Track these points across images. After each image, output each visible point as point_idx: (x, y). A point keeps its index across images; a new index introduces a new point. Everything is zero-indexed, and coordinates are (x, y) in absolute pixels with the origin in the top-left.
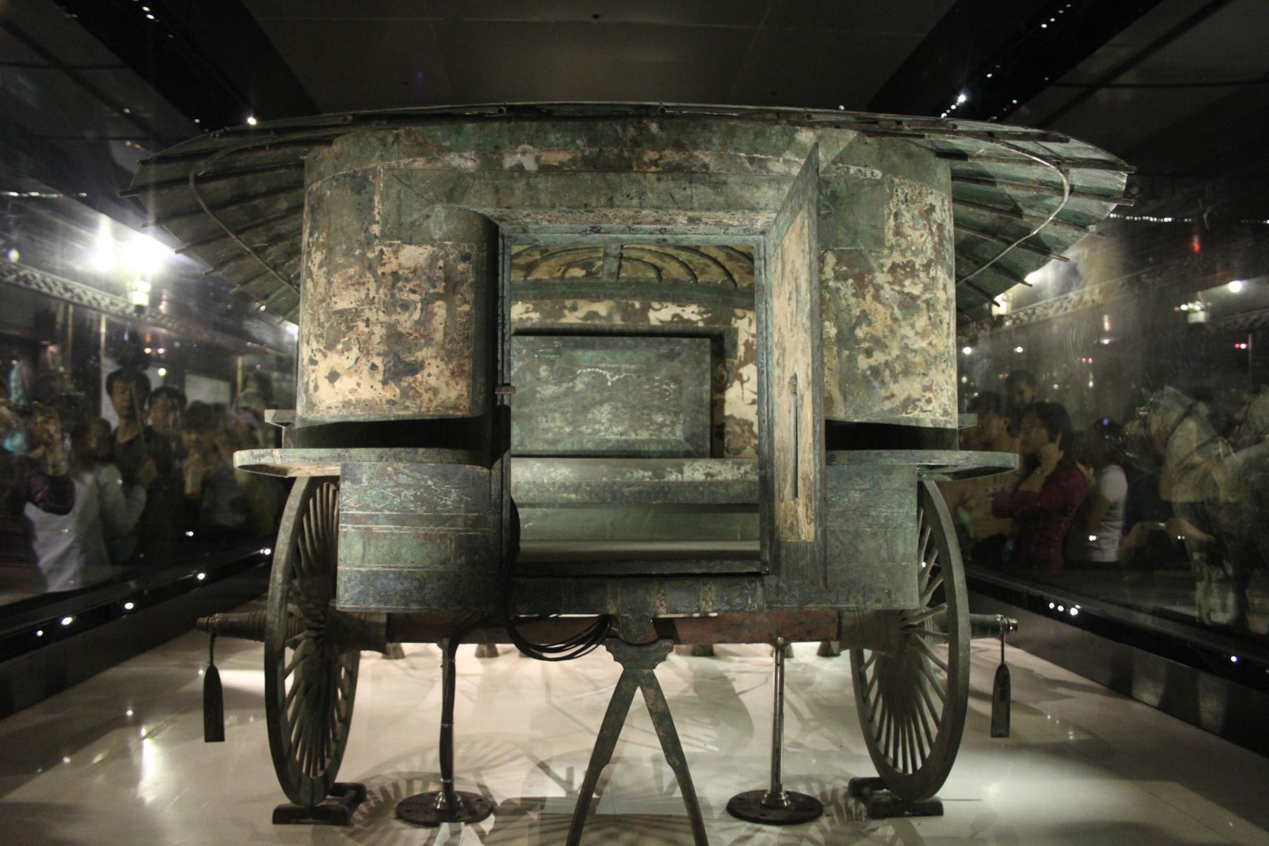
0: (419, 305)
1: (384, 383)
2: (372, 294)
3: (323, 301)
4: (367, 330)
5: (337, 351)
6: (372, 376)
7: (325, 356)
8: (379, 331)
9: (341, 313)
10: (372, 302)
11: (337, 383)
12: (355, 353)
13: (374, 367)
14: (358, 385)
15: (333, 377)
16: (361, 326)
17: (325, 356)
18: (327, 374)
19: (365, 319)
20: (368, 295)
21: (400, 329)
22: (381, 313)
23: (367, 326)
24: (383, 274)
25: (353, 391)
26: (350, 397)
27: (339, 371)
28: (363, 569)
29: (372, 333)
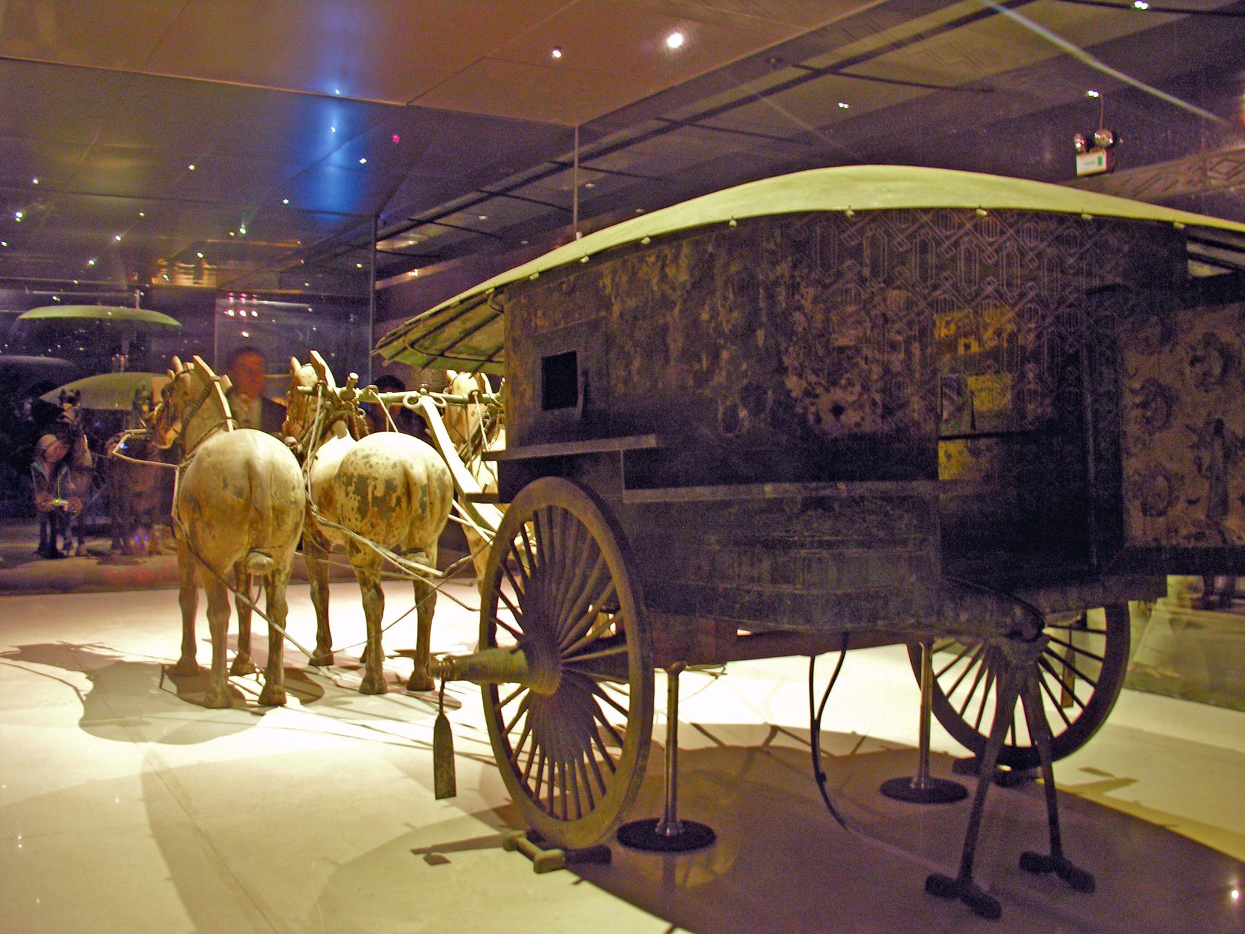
0: (903, 347)
1: (883, 417)
2: (869, 333)
3: (821, 335)
4: (865, 366)
5: (840, 386)
6: (874, 412)
7: (827, 390)
8: (876, 370)
9: (841, 350)
10: (868, 341)
11: (843, 417)
12: (858, 388)
13: (874, 403)
14: (862, 419)
15: (837, 410)
16: (862, 363)
17: (827, 390)
18: (830, 407)
19: (864, 356)
20: (865, 334)
21: (891, 367)
22: (876, 352)
23: (866, 363)
24: (876, 315)
25: (858, 425)
26: (855, 430)
27: (844, 404)
28: (839, 592)
29: (870, 371)
